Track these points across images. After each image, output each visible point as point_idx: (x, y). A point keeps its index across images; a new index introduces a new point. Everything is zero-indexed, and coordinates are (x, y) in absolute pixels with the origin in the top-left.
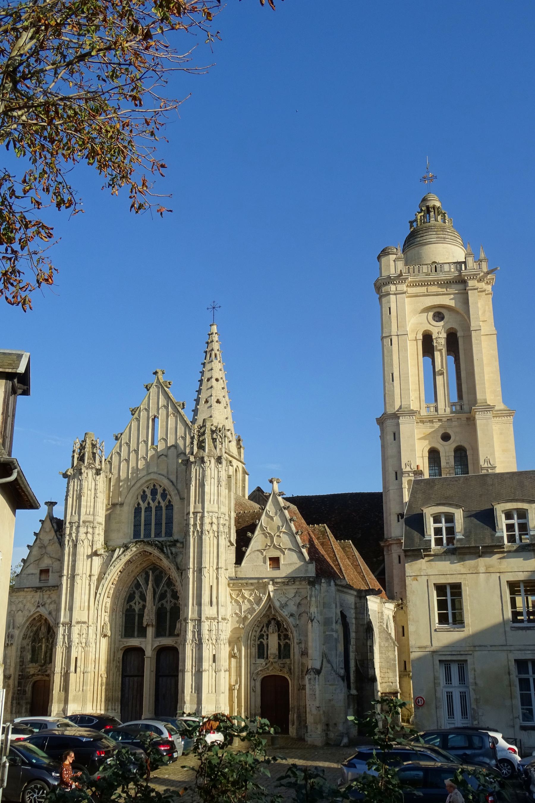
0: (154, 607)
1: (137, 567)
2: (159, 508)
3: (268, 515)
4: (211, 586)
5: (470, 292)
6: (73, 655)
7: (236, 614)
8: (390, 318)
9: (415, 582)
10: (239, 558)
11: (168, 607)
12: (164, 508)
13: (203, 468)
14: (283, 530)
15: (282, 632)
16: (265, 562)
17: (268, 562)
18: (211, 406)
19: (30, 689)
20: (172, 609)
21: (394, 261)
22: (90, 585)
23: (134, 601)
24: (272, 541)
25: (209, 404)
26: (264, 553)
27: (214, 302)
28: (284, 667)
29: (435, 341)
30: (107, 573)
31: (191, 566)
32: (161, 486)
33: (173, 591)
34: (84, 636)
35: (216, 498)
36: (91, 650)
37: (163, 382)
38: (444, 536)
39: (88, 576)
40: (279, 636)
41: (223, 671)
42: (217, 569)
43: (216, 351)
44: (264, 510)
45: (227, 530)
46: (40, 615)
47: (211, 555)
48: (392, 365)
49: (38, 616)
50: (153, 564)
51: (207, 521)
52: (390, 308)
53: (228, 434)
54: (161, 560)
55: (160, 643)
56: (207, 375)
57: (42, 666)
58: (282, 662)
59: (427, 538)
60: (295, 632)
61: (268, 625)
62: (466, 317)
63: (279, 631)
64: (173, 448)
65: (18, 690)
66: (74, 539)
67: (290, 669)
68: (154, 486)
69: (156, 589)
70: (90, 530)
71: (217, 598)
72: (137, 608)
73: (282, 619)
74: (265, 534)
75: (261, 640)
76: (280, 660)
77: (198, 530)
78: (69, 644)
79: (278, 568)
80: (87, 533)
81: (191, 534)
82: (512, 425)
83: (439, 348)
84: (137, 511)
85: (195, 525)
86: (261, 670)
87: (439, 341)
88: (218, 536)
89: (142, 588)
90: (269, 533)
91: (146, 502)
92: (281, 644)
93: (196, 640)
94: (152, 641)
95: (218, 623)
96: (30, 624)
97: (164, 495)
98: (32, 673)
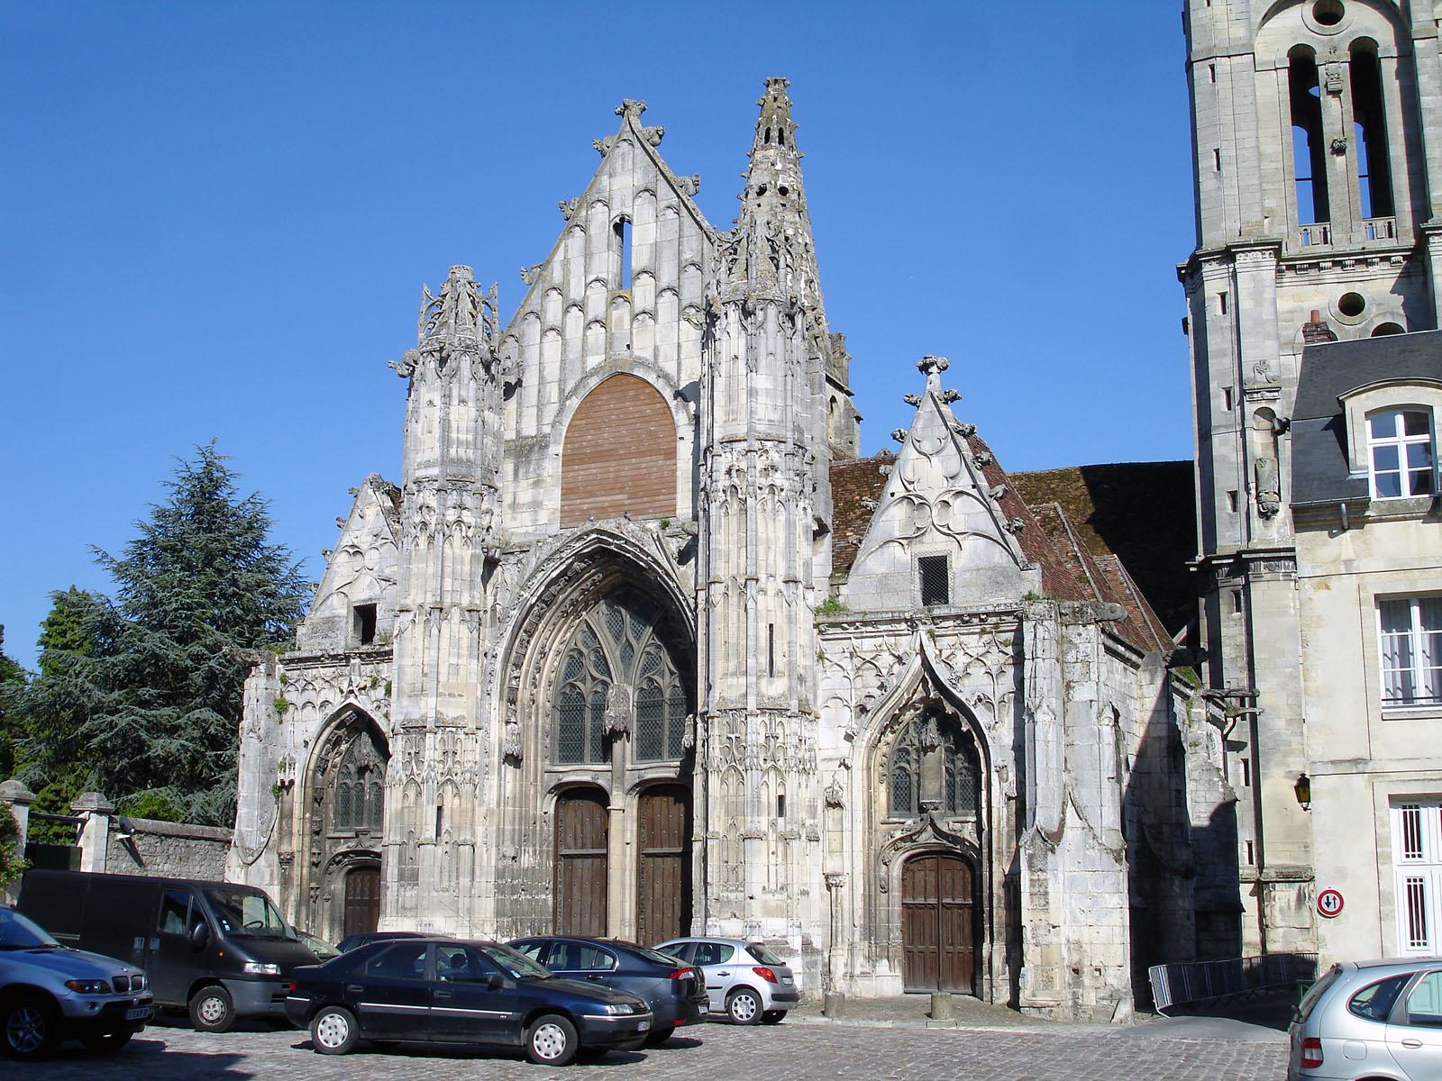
4: (771, 626)
9: (1324, 592)
10: (844, 563)
29: (1321, 70)
38: (1404, 471)
41: (804, 837)
59: (1356, 474)
64: (669, 293)
70: (468, 500)
86: (901, 839)
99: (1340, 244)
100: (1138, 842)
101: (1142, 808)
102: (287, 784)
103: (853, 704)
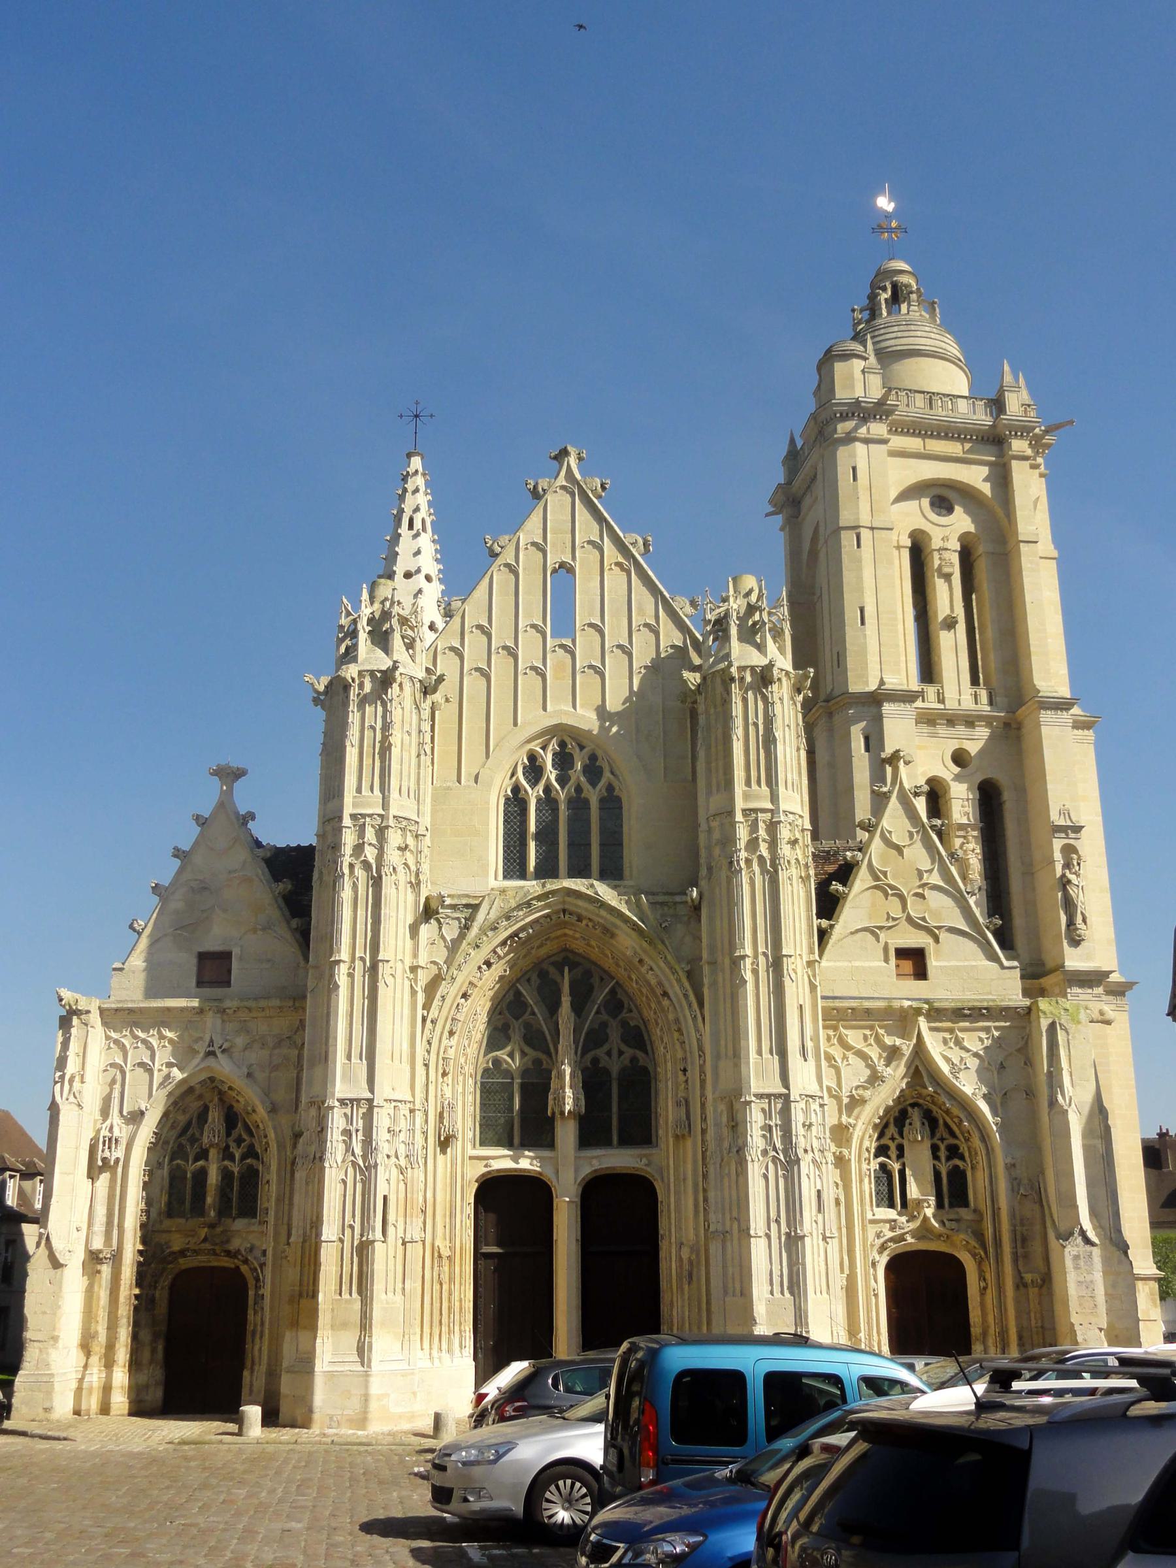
2: (578, 804)
3: (888, 843)
5: (1014, 463)
6: (382, 1189)
8: (856, 489)
11: (615, 1067)
13: (765, 699)
15: (942, 1140)
16: (886, 960)
19: (166, 1293)
20: (623, 1070)
21: (863, 372)
26: (882, 935)
27: (417, 403)
29: (936, 555)
30: (456, 964)
32: (582, 747)
33: (624, 1024)
34: (402, 1136)
40: (935, 1149)
48: (860, 590)
50: (566, 950)
52: (854, 469)
57: (212, 1226)
62: (1000, 512)
63: (933, 1135)
66: (372, 860)
67: (979, 1236)
68: (562, 744)
70: (410, 841)
74: (881, 887)
75: (881, 1159)
76: (941, 1212)
77: (761, 858)
78: (365, 1157)
79: (921, 973)
80: (403, 849)
82: (1092, 747)
83: (946, 570)
84: (516, 803)
85: (753, 844)
87: (946, 555)
91: (540, 788)
93: (775, 1149)
94: (576, 1157)
95: (822, 1106)
97: (593, 771)
98: (176, 1248)
99: (951, 704)
103: (845, 1093)
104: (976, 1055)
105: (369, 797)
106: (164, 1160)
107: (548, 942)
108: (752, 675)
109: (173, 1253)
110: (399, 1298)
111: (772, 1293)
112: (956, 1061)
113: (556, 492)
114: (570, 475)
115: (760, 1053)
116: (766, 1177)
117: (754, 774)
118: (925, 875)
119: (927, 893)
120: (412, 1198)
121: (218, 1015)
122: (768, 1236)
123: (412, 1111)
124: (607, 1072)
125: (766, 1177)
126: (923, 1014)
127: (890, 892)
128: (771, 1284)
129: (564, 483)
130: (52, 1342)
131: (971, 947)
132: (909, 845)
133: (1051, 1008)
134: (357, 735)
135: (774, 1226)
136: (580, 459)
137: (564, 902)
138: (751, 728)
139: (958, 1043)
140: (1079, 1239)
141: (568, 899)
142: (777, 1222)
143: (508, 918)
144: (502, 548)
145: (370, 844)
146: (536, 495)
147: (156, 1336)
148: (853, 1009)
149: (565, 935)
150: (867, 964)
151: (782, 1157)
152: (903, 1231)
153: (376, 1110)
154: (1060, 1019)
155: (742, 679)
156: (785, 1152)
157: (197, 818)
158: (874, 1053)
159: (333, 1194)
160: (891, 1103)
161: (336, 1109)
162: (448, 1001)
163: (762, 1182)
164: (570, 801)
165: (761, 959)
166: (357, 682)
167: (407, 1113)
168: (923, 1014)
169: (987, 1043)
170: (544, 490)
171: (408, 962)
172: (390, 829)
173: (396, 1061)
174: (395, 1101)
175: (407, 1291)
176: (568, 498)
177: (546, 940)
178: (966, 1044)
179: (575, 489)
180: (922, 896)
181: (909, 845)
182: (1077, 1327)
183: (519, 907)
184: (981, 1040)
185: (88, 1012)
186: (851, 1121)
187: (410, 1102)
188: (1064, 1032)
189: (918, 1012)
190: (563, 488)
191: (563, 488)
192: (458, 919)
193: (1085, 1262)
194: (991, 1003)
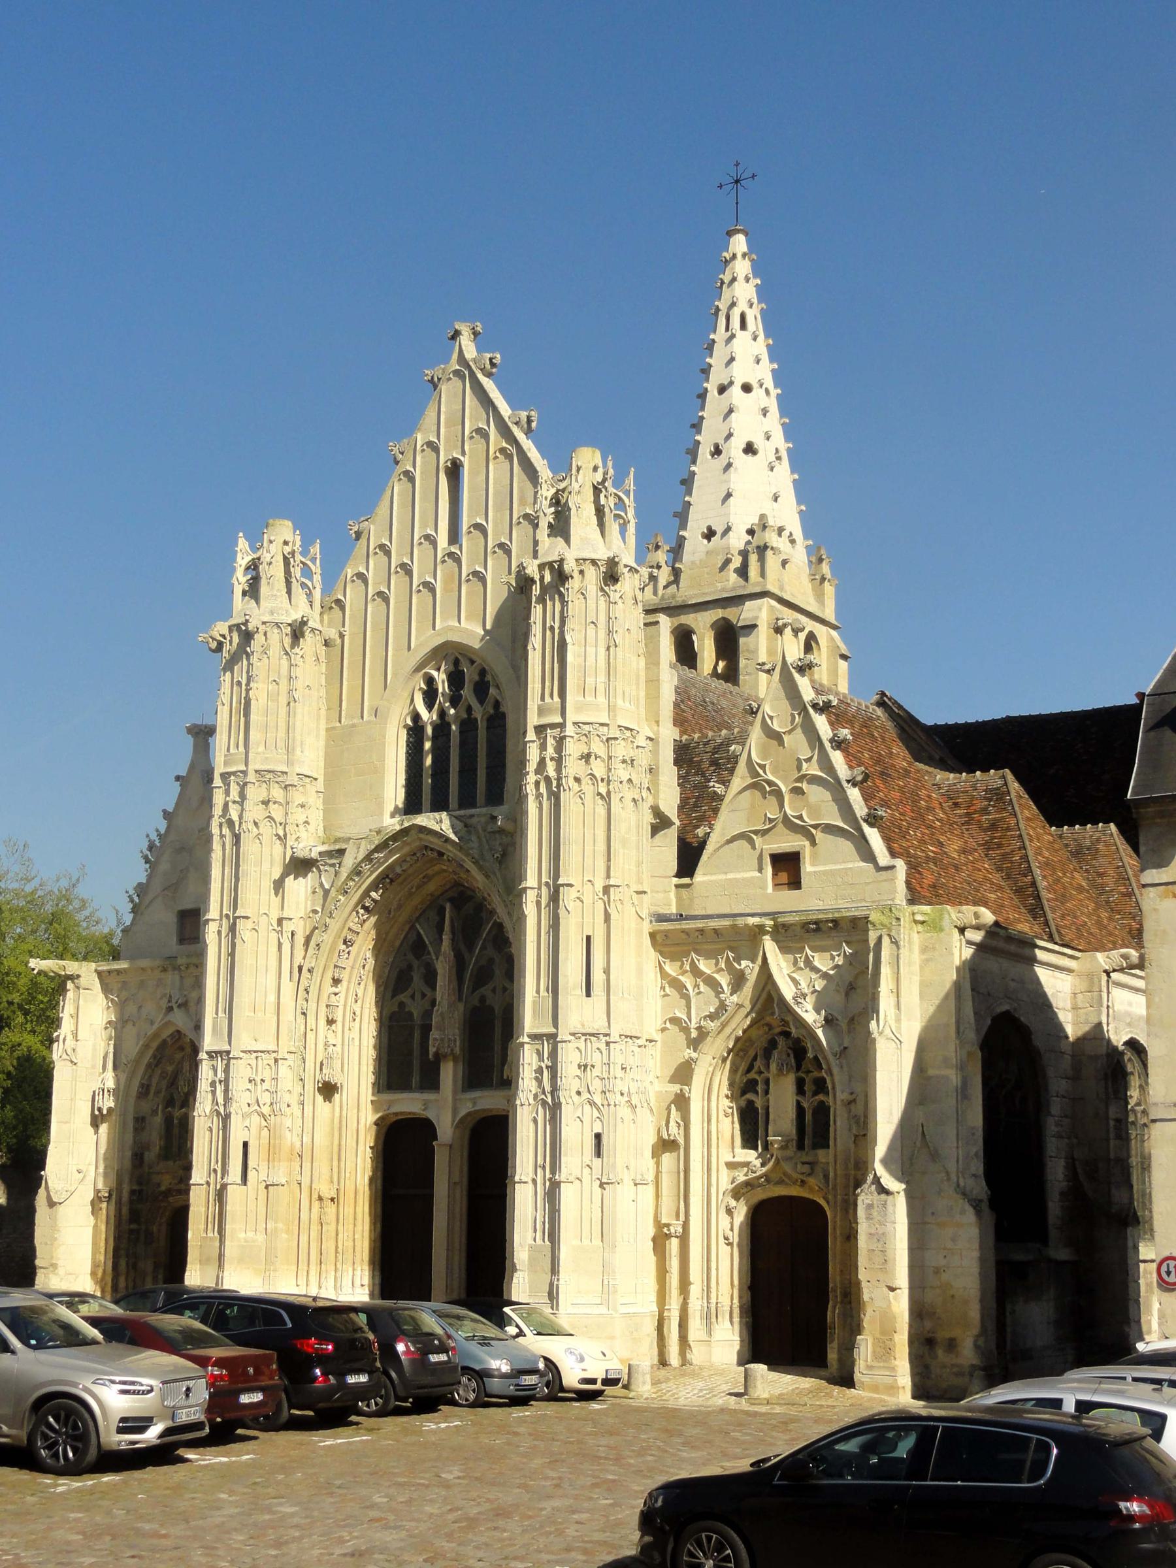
0: (461, 1007)
1: (411, 894)
2: (468, 725)
4: (589, 938)
7: (674, 1020)
12: (482, 725)
13: (561, 595)
14: (814, 770)
17: (769, 870)
18: (729, 465)
19: (164, 1228)
22: (280, 945)
23: (410, 991)
24: (781, 806)
25: (722, 460)
27: (737, 165)
28: (809, 1175)
31: (531, 881)
34: (266, 1086)
35: (602, 678)
36: (288, 1123)
37: (474, 360)
39: (275, 923)
42: (606, 889)
43: (742, 306)
44: (756, 713)
45: (643, 779)
46: (178, 1031)
47: (589, 848)
49: (172, 1035)
50: (457, 884)
51: (573, 748)
53: (781, 543)
54: (468, 871)
55: (475, 1104)
56: (717, 377)
58: (805, 1159)
60: (835, 1070)
61: (768, 1053)
63: (798, 1068)
65: (131, 1231)
66: (235, 817)
67: (826, 1177)
68: (457, 662)
69: (466, 955)
70: (277, 793)
71: (607, 971)
72: (416, 1011)
73: (803, 1032)
74: (758, 786)
75: (750, 1096)
76: (799, 1154)
77: (548, 779)
79: (795, 883)
81: (530, 789)
88: (609, 793)
89: (429, 953)
90: (770, 783)
92: (805, 1105)
93: (544, 1093)
94: (455, 1100)
95: (608, 1044)
96: (154, 1056)
97: (481, 689)
98: (163, 1188)
100: (1068, 1181)
101: (1075, 1141)
102: (105, 1112)
103: (694, 1025)
104: (825, 976)
105: (235, 754)
106: (158, 1108)
107: (425, 880)
108: (551, 573)
109: (164, 1192)
110: (261, 1238)
111: (535, 1240)
112: (803, 984)
113: (450, 379)
114: (462, 359)
115: (538, 992)
116: (535, 1121)
117: (547, 684)
118: (805, 765)
119: (805, 786)
120: (274, 1144)
121: (176, 972)
122: (534, 1181)
123: (276, 1060)
124: (492, 1009)
125: (535, 1121)
126: (767, 933)
127: (768, 789)
128: (535, 1231)
129: (458, 367)
130: (51, 1269)
131: (847, 846)
132: (790, 732)
133: (882, 918)
134: (228, 692)
135: (539, 1171)
136: (476, 334)
137: (421, 839)
138: (548, 633)
139: (808, 963)
140: (873, 1187)
141: (421, 836)
142: (544, 1168)
143: (371, 860)
144: (402, 453)
145: (234, 802)
146: (434, 384)
147: (156, 1266)
148: (701, 931)
149: (445, 871)
150: (739, 876)
151: (549, 1100)
152: (754, 1175)
153: (232, 1061)
154: (890, 929)
155: (542, 578)
156: (552, 1093)
157: (178, 778)
158: (724, 980)
159: (201, 1142)
160: (741, 1033)
161: (204, 1063)
162: (325, 948)
163: (532, 1125)
164: (436, 728)
165: (544, 889)
166: (228, 638)
167: (272, 1062)
168: (768, 932)
169: (840, 961)
170: (439, 379)
171: (275, 915)
172: (249, 785)
173: (260, 1014)
174: (255, 1052)
175: (268, 1231)
176: (460, 383)
177: (424, 877)
178: (817, 963)
179: (465, 371)
180: (798, 791)
181: (790, 732)
182: (864, 1284)
183: (377, 849)
184: (833, 958)
185: (78, 976)
186: (694, 1055)
187: (274, 1052)
188: (894, 946)
189: (761, 929)
190: (457, 373)
191: (457, 373)
192: (333, 865)
193: (879, 1212)
194: (837, 915)
